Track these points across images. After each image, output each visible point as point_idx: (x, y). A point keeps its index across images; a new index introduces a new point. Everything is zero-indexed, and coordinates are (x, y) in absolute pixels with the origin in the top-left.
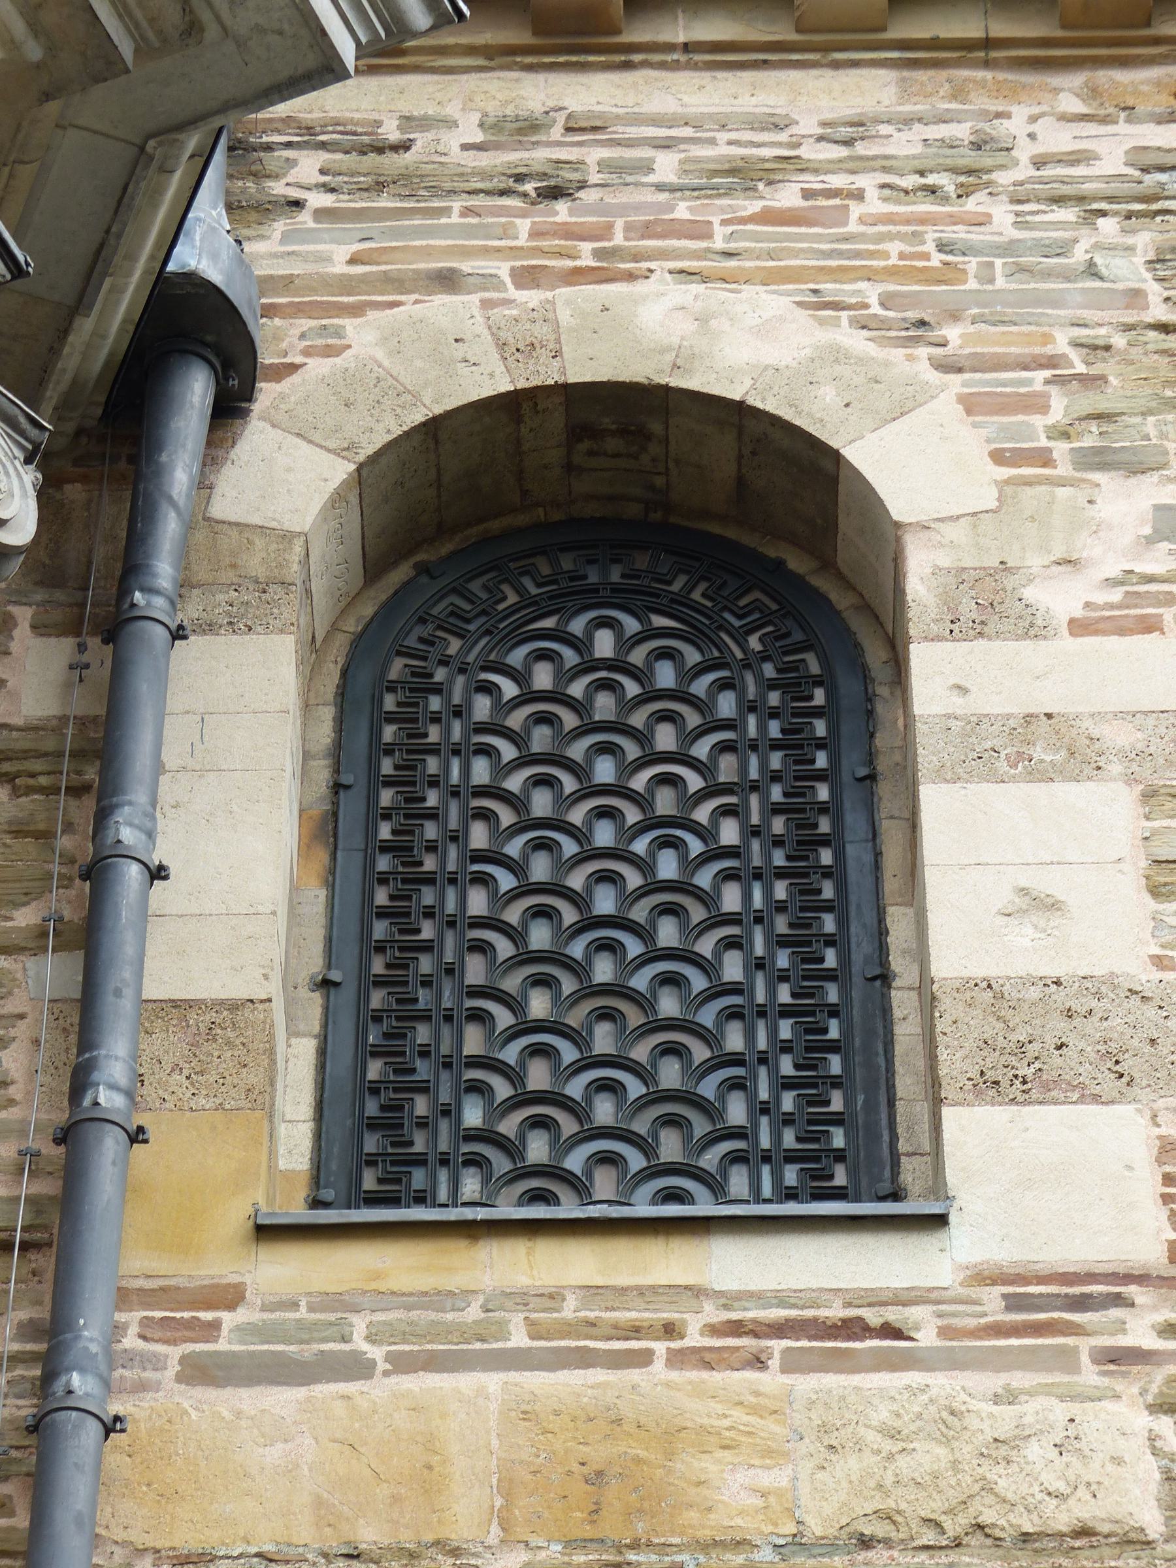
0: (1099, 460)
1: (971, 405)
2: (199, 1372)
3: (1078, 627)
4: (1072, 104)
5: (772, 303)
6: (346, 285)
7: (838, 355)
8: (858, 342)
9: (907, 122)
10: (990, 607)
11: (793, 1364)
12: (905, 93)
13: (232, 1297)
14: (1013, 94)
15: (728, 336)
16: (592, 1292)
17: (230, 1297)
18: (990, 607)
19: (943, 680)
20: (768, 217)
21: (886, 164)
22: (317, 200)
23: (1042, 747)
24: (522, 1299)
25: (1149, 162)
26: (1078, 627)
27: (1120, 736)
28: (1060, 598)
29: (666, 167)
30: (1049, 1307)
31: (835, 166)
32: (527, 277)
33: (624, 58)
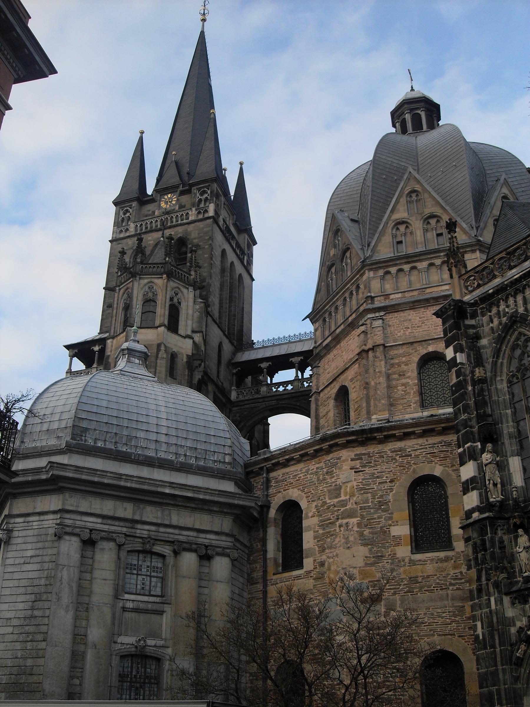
0: (312, 501)
1: (306, 497)
2: (272, 585)
3: (311, 517)
4: (313, 463)
5: (296, 490)
6: (275, 493)
7: (299, 494)
8: (300, 492)
9: (304, 468)
10: (307, 517)
11: (297, 580)
12: (305, 464)
13: (272, 579)
14: (311, 463)
15: (294, 494)
16: (288, 576)
17: (272, 579)
18: (307, 517)
19: (305, 523)
20: (297, 480)
21: (303, 473)
22: (274, 485)
23: (309, 528)
24: (284, 577)
25: (317, 468)
26: (311, 517)
27: (313, 526)
28: (310, 514)
29: (291, 476)
30: (309, 572)
31: (301, 474)
32: (284, 490)
33: (289, 466)
